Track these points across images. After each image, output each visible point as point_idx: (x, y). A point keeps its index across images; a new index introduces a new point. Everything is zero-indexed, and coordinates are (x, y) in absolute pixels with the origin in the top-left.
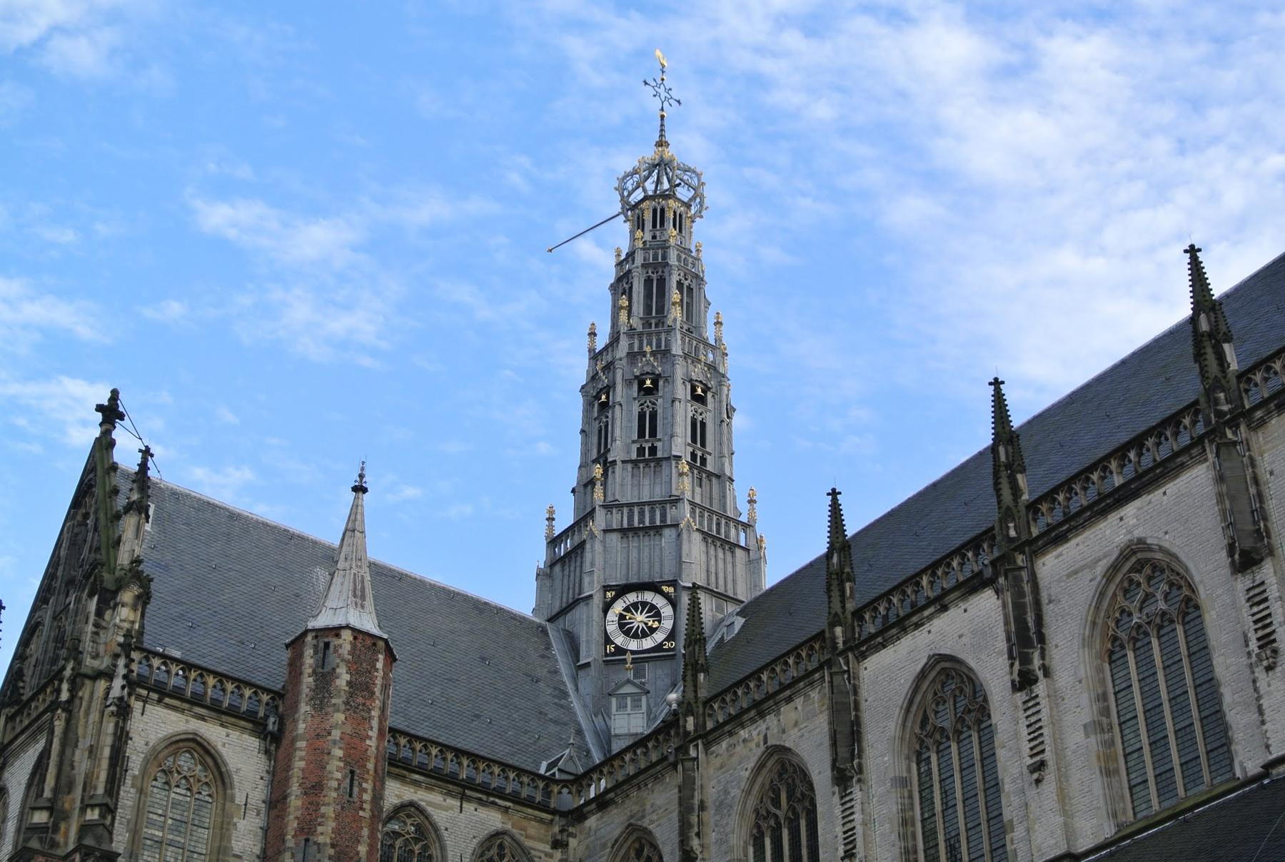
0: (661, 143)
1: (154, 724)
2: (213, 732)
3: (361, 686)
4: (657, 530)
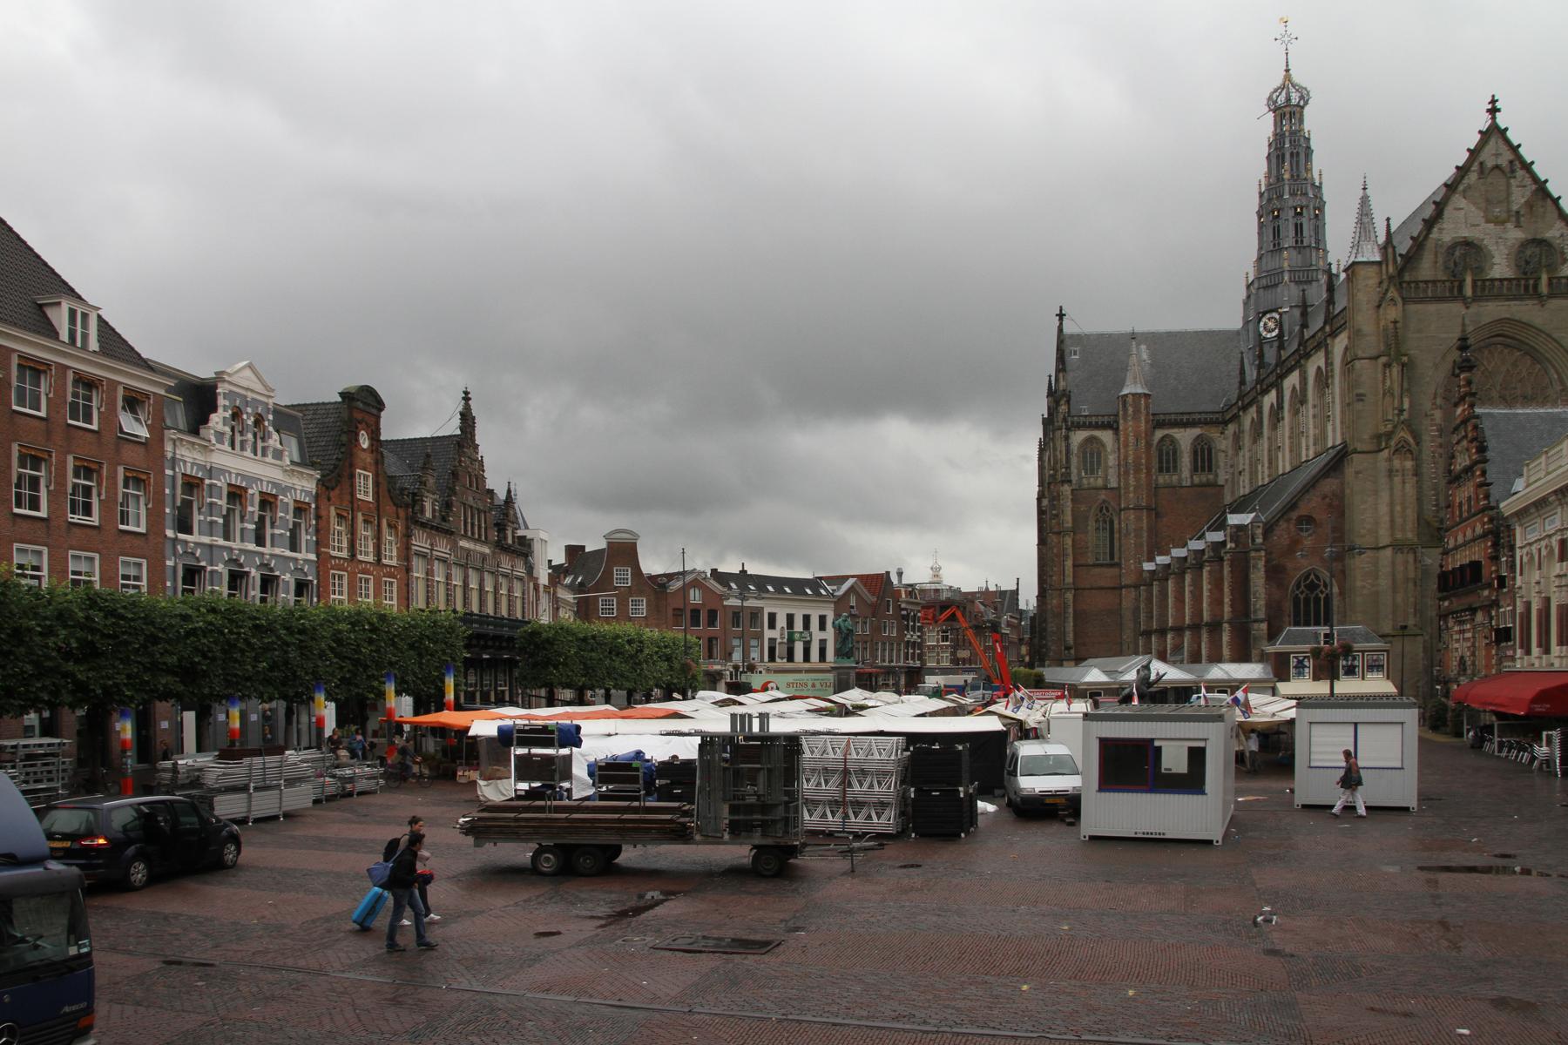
0: (1287, 70)
1: (1078, 437)
2: (1097, 433)
3: (1137, 411)
4: (1276, 285)
